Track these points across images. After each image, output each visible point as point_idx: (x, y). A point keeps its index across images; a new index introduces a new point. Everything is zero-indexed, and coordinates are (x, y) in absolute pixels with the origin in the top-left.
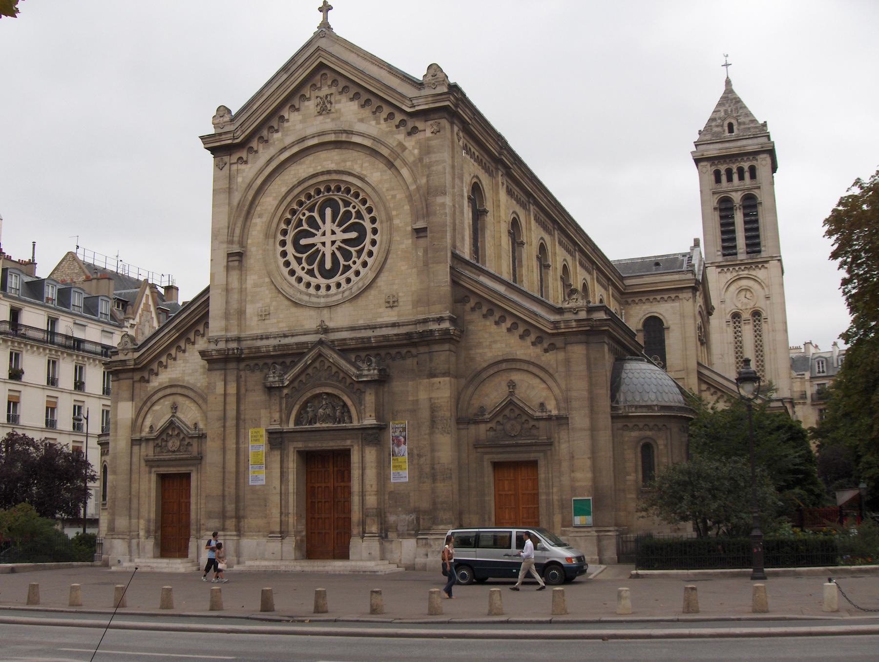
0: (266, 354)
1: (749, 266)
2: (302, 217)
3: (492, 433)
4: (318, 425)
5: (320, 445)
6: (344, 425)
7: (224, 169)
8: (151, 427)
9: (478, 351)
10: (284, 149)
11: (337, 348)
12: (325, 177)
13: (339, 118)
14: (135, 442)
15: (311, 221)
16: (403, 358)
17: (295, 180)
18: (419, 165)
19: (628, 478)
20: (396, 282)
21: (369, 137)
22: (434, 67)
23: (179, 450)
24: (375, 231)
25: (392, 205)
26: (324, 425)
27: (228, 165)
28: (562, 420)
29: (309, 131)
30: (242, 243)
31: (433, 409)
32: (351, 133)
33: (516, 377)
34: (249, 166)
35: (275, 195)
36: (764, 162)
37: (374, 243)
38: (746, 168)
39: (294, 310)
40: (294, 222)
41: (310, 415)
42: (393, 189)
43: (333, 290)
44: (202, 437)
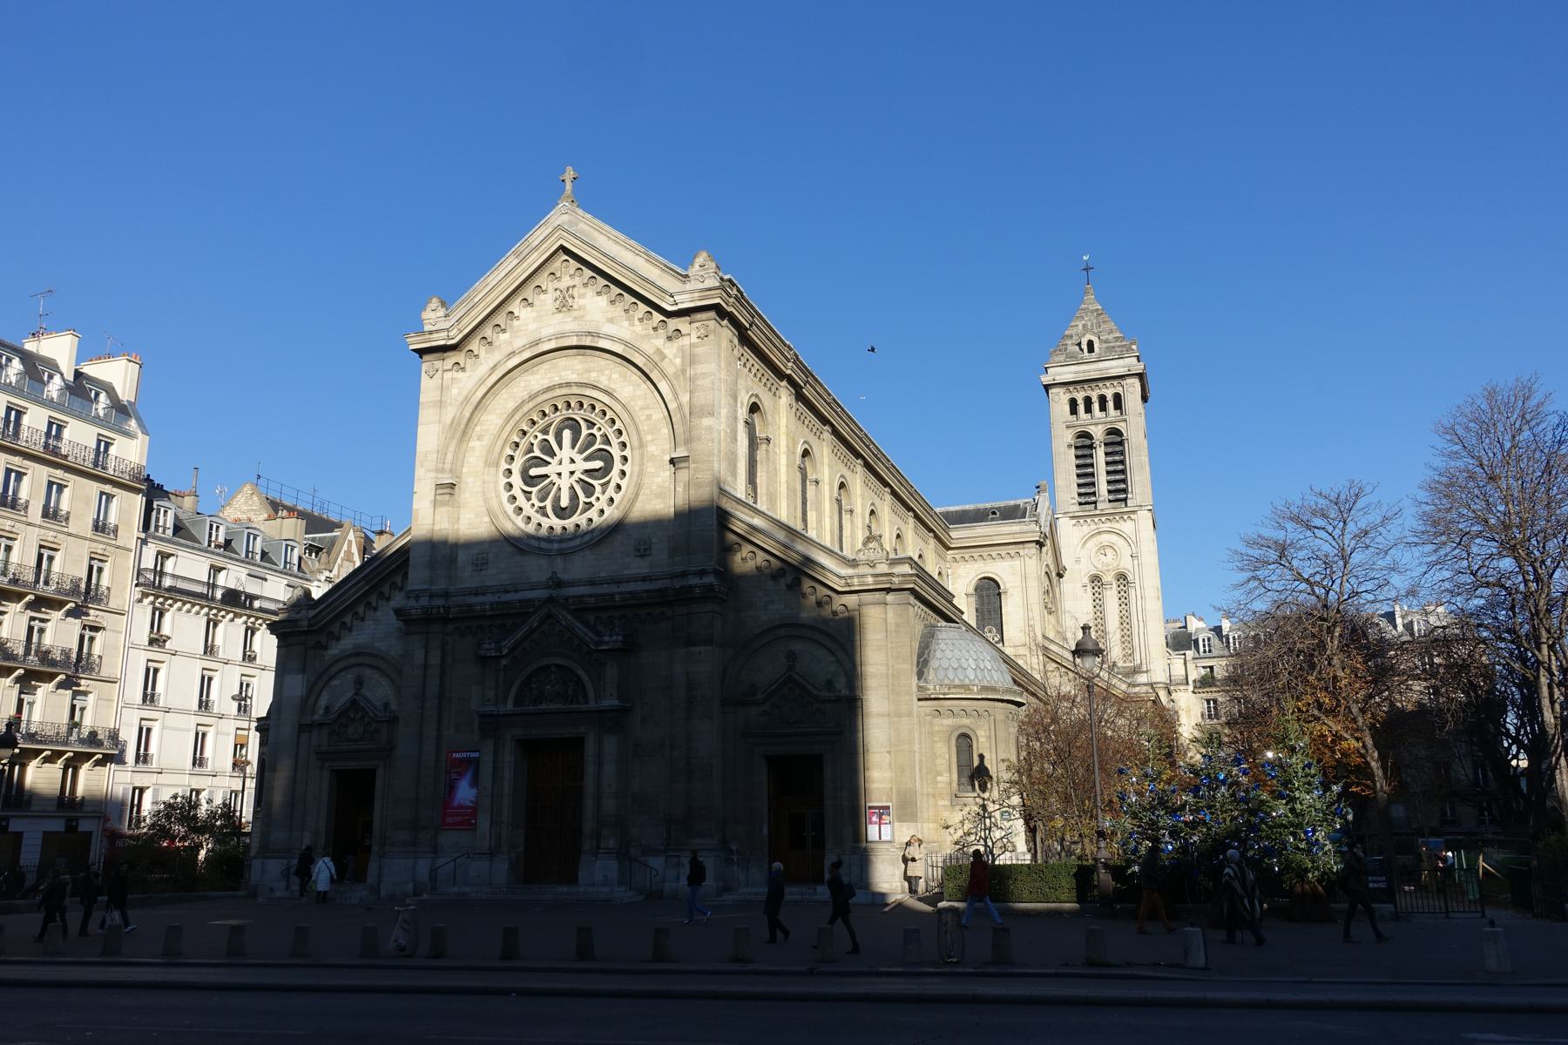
1: (1110, 516)
2: (533, 441)
4: (544, 706)
8: (327, 708)
11: (573, 607)
12: (564, 391)
13: (583, 317)
14: (303, 728)
17: (526, 393)
18: (681, 378)
19: (939, 778)
24: (625, 459)
25: (646, 428)
26: (552, 706)
27: (440, 371)
29: (545, 332)
33: (797, 647)
34: (467, 374)
35: (498, 412)
36: (1131, 390)
38: (1110, 397)
42: (648, 407)
44: (394, 720)
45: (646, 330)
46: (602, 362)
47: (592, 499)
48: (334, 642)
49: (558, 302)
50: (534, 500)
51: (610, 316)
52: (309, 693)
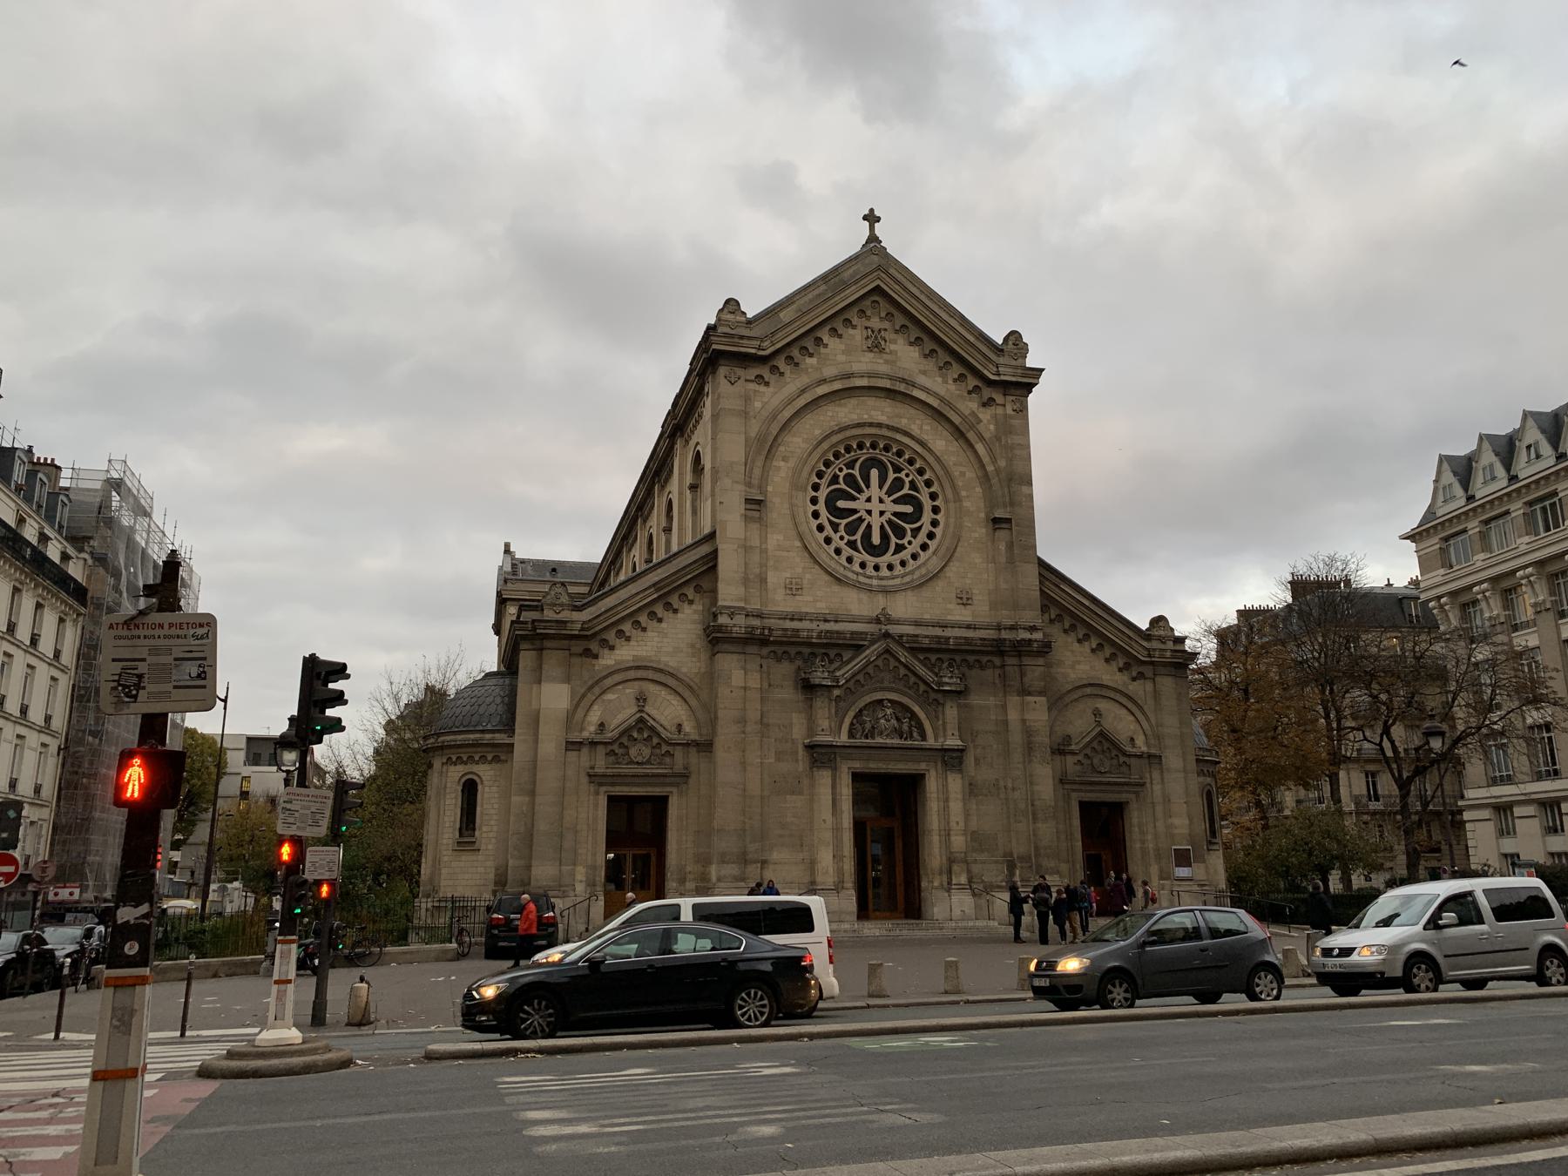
3: (1078, 768)
8: (602, 725)
9: (1059, 670)
10: (823, 381)
15: (850, 479)
16: (982, 668)
17: (833, 423)
21: (936, 395)
22: (1016, 335)
23: (648, 762)
24: (936, 510)
25: (960, 484)
26: (888, 741)
28: (1154, 759)
29: (856, 368)
30: (762, 488)
31: (1028, 732)
33: (1103, 705)
35: (805, 436)
37: (935, 523)
39: (836, 588)
41: (868, 726)
42: (961, 465)
46: (913, 411)
48: (606, 651)
49: (870, 343)
52: (577, 706)
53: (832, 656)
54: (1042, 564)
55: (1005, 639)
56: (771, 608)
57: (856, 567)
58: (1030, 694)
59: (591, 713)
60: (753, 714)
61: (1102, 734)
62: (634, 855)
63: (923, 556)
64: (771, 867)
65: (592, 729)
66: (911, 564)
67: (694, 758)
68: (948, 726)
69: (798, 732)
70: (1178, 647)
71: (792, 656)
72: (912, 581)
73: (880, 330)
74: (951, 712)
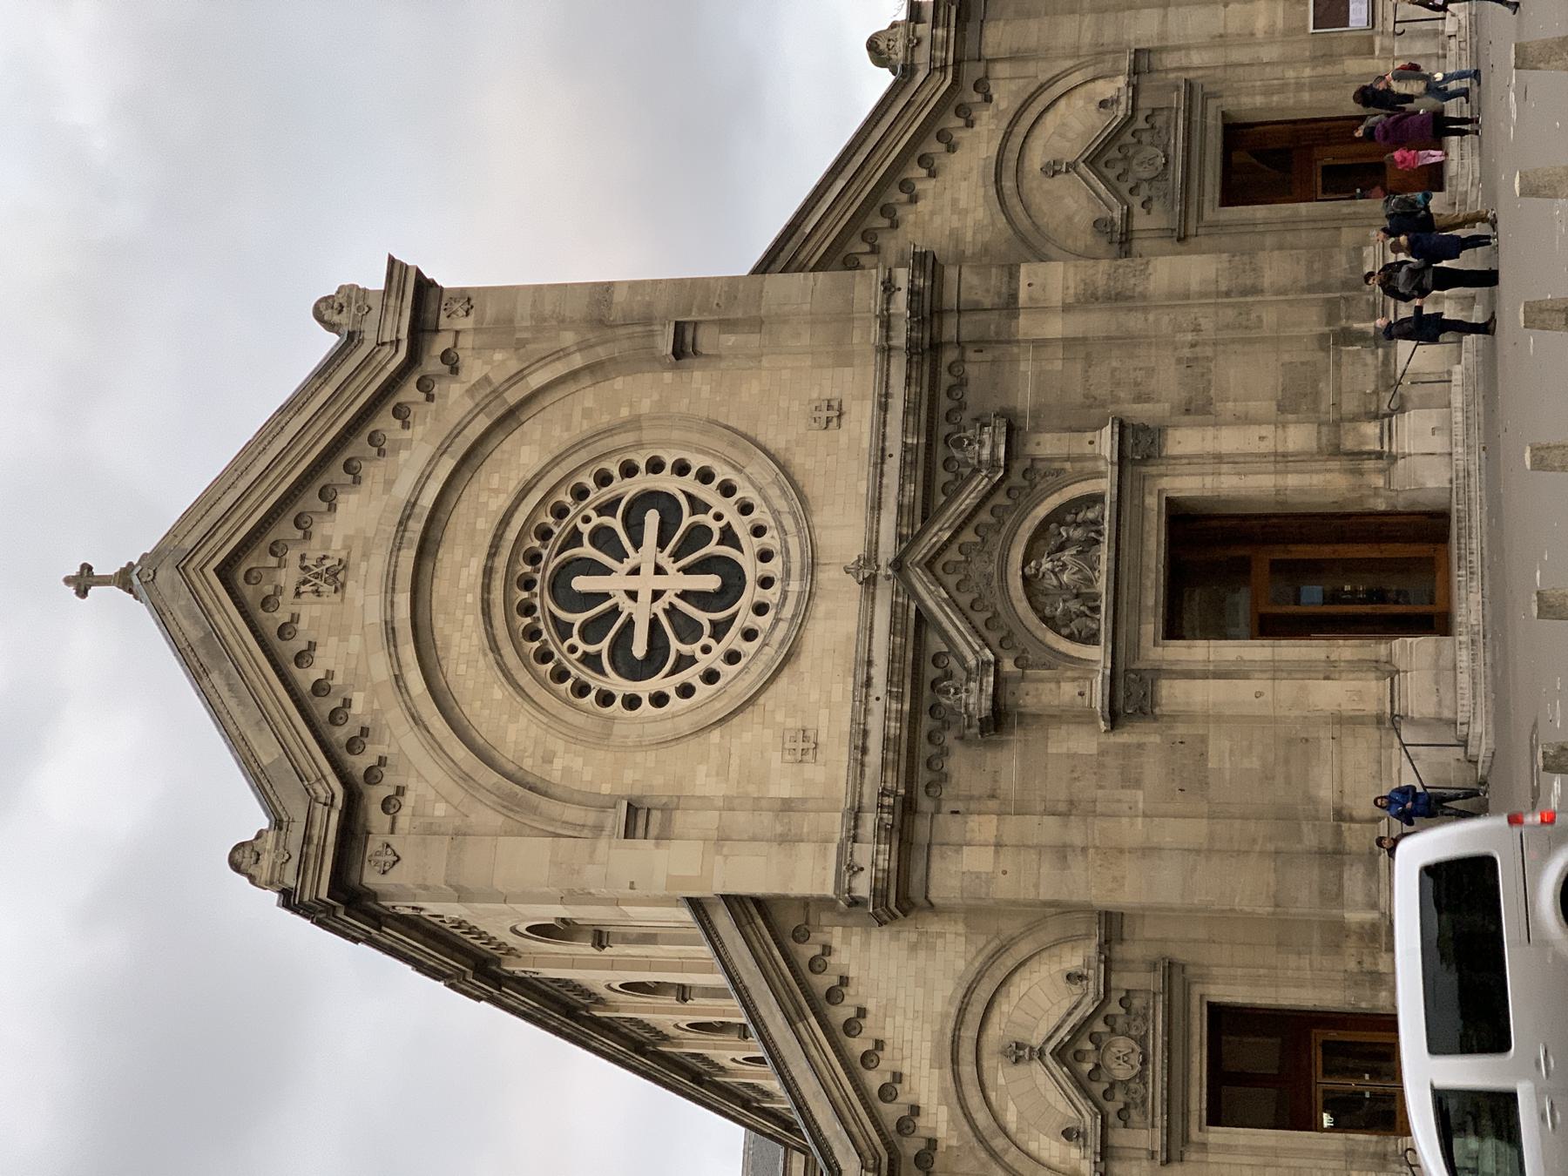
0: (905, 725)
3: (1156, 206)
5: (1153, 576)
6: (1107, 513)
7: (398, 853)
8: (1067, 1134)
15: (591, 631)
16: (962, 383)
17: (482, 663)
20: (783, 404)
21: (433, 461)
22: (323, 306)
23: (1142, 1041)
24: (655, 466)
26: (1103, 567)
27: (392, 840)
29: (375, 616)
31: (1088, 299)
32: (412, 505)
33: (1036, 158)
34: (412, 784)
35: (506, 717)
37: (682, 469)
39: (804, 662)
40: (588, 675)
41: (1074, 606)
43: (774, 568)
45: (426, 417)
46: (462, 508)
47: (716, 527)
48: (921, 1121)
49: (325, 588)
50: (694, 649)
51: (381, 486)
53: (939, 673)
54: (766, 265)
55: (909, 339)
56: (841, 792)
57: (763, 622)
58: (1014, 296)
59: (1044, 1155)
60: (1048, 829)
61: (1092, 161)
62: (1327, 1072)
63: (744, 492)
64: (1347, 802)
65: (1075, 1153)
66: (760, 515)
67: (1131, 951)
68: (1076, 451)
69: (1084, 742)
70: (928, 14)
71: (936, 751)
72: (794, 514)
73: (304, 568)
74: (1048, 445)
